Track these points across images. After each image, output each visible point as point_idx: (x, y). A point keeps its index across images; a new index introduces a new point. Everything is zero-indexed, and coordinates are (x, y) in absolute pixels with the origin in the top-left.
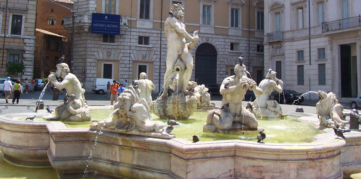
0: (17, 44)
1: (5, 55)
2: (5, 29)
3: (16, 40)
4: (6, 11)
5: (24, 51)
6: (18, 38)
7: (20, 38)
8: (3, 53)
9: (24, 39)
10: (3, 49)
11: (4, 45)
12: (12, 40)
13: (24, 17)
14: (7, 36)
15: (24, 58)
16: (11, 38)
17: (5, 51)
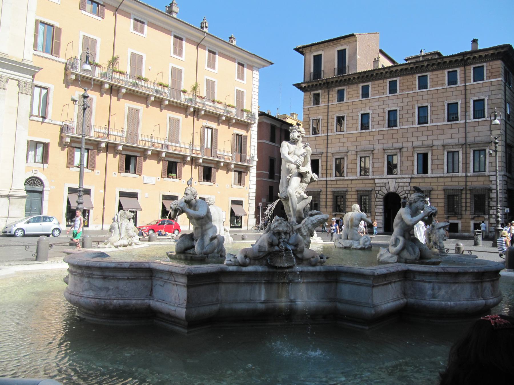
0: (481, 183)
1: (468, 196)
2: (466, 168)
3: (480, 179)
4: (466, 148)
5: (490, 190)
6: (482, 176)
7: (485, 176)
8: (466, 194)
9: (489, 176)
10: (466, 190)
11: (466, 185)
12: (475, 179)
13: (487, 151)
14: (469, 174)
15: (491, 198)
16: (473, 176)
17: (468, 192)
